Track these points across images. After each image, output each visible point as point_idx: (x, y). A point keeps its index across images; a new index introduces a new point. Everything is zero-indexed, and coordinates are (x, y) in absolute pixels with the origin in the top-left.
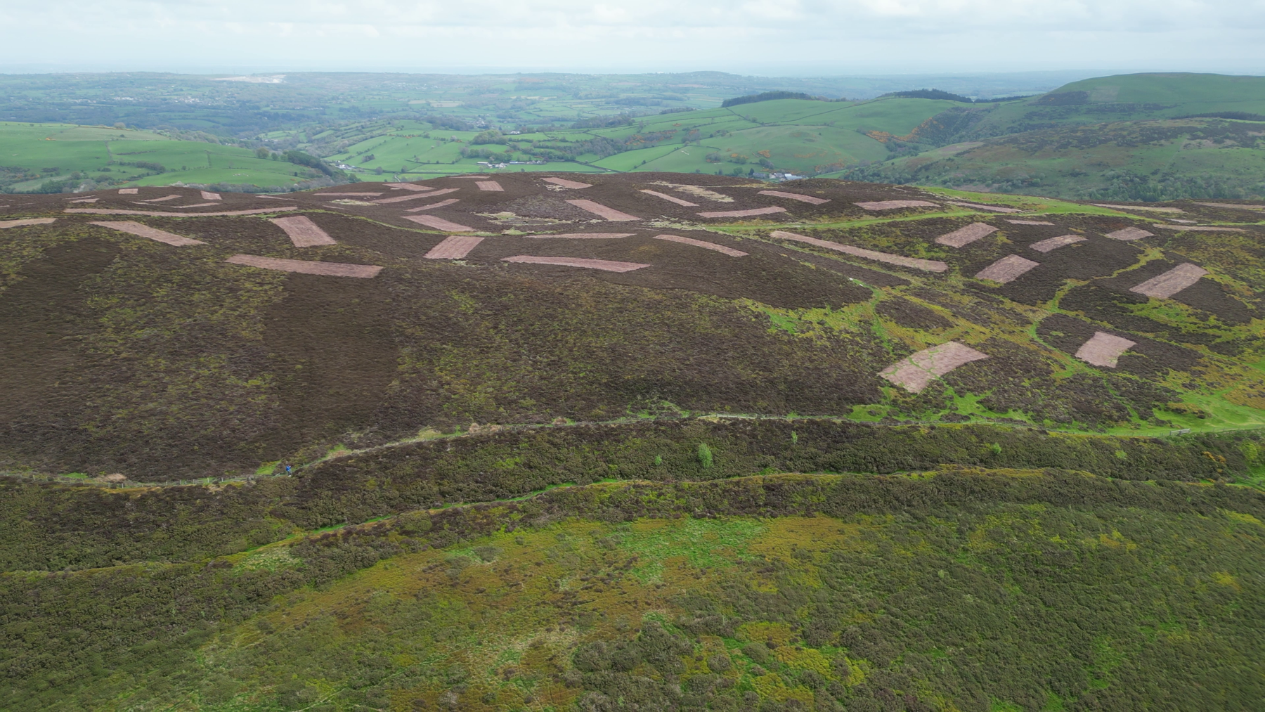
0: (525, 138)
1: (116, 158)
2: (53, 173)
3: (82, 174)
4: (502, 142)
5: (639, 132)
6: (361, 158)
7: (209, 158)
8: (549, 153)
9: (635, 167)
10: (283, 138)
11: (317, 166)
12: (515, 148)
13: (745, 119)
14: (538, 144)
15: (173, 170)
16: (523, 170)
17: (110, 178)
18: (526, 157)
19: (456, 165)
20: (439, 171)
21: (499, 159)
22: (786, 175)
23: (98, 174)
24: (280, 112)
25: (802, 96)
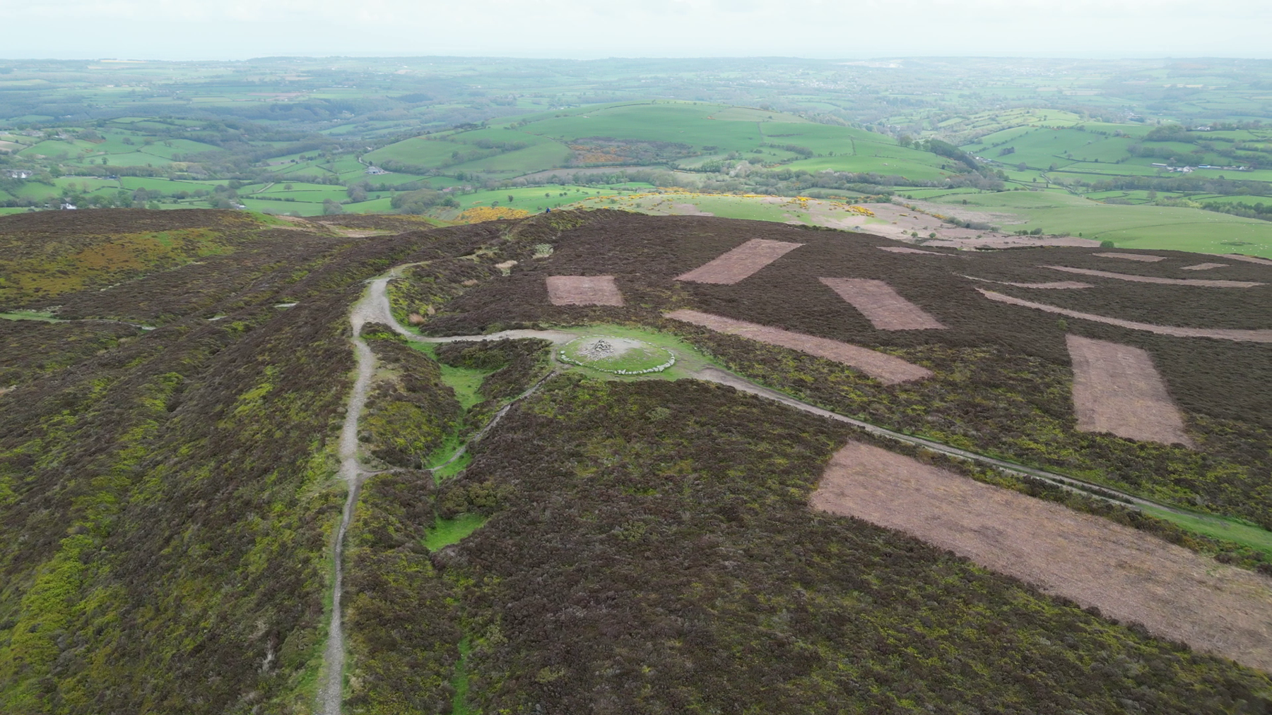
0: (1222, 136)
1: (768, 140)
2: (712, 151)
3: (737, 154)
4: (1189, 141)
6: (999, 149)
7: (853, 144)
8: (1260, 157)
10: (905, 125)
11: (962, 157)
12: (1208, 149)
15: (820, 156)
16: (1222, 177)
17: (762, 161)
18: (1224, 160)
19: (1120, 166)
20: (1098, 171)
21: (1182, 161)
23: (751, 156)
24: (900, 97)
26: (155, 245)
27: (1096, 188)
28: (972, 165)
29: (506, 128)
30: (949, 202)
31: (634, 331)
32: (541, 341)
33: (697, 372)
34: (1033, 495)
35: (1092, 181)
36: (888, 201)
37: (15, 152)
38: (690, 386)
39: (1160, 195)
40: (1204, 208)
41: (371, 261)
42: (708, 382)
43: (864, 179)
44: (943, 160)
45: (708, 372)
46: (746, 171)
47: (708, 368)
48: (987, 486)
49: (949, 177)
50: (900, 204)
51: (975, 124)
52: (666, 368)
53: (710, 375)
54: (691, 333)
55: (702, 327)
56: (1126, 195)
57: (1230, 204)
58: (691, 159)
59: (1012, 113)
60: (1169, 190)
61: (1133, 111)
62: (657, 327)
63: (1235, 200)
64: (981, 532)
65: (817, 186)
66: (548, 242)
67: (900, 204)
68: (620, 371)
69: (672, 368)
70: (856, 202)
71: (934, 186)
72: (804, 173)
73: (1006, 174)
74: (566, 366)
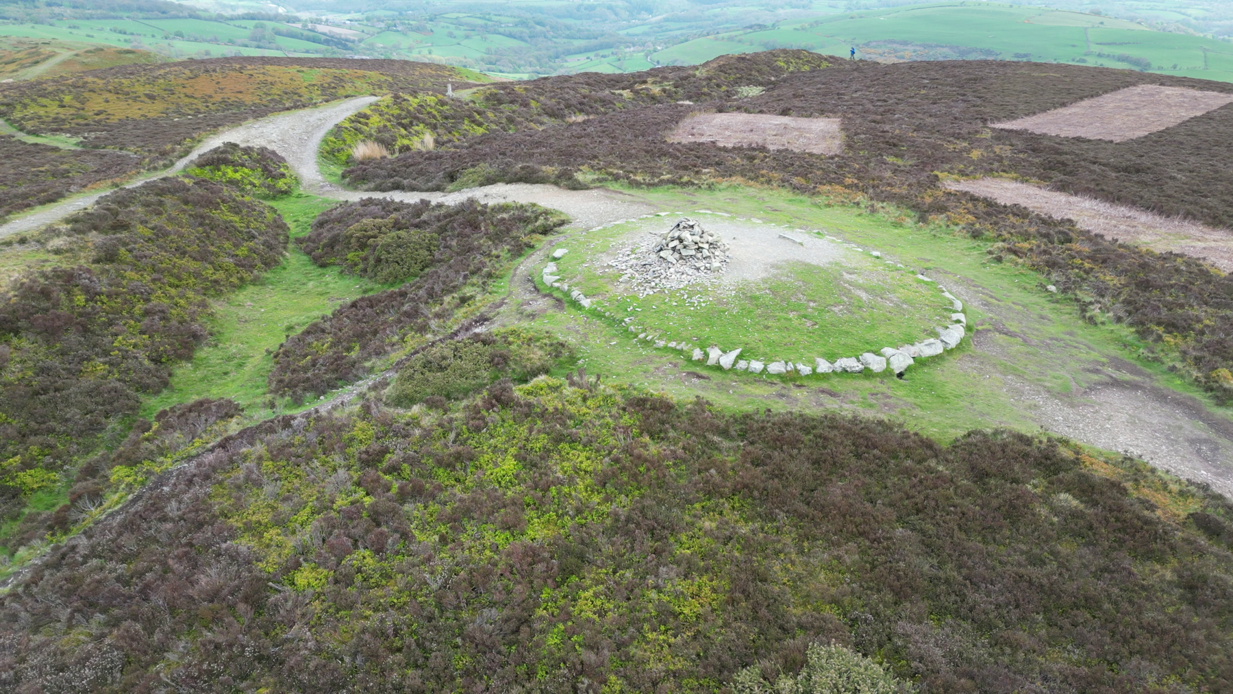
7: (1205, 57)
26: (291, 79)
31: (838, 210)
33: (1065, 396)
37: (360, 41)
38: (1034, 485)
42: (1136, 470)
45: (1118, 406)
47: (1116, 384)
52: (920, 362)
53: (1132, 422)
54: (1027, 237)
55: (1062, 222)
62: (915, 207)
66: (761, 84)
68: (714, 354)
69: (952, 364)
74: (541, 303)
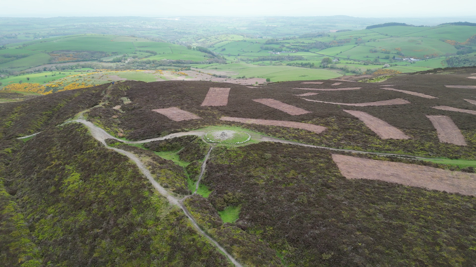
1: (138, 49)
2: (116, 54)
3: (127, 55)
5: (335, 39)
6: (221, 49)
7: (171, 49)
8: (298, 48)
9: (337, 54)
10: (186, 41)
11: (210, 53)
13: (381, 34)
14: (293, 44)
15: (160, 54)
16: (289, 55)
18: (288, 50)
19: (259, 53)
20: (253, 55)
21: (277, 50)
22: (411, 59)
23: (133, 55)
24: (182, 31)
25: (404, 25)
27: (254, 61)
28: (213, 54)
29: (17, 48)
30: (211, 69)
32: (193, 136)
34: (393, 161)
35: (252, 58)
36: (190, 70)
39: (273, 62)
40: (287, 65)
41: (44, 113)
43: (178, 62)
44: (204, 54)
46: (132, 61)
48: (378, 161)
49: (208, 60)
50: (194, 71)
51: (211, 40)
56: (263, 63)
57: (294, 63)
58: (107, 57)
59: (222, 36)
60: (275, 60)
61: (258, 34)
63: (295, 62)
64: (393, 175)
65: (162, 65)
67: (194, 71)
70: (179, 71)
71: (203, 63)
72: (156, 61)
73: (225, 58)
